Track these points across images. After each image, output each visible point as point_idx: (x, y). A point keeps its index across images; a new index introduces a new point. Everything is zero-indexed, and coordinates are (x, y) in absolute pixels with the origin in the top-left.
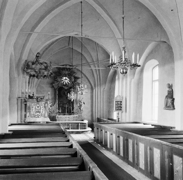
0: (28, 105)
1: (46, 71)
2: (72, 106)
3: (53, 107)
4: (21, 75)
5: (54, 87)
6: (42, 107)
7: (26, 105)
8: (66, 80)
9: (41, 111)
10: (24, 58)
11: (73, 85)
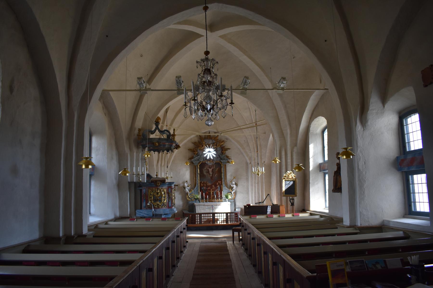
0: (144, 191)
1: (167, 142)
4: (135, 150)
5: (193, 163)
6: (163, 193)
7: (141, 190)
8: (210, 153)
9: (163, 199)
10: (139, 124)
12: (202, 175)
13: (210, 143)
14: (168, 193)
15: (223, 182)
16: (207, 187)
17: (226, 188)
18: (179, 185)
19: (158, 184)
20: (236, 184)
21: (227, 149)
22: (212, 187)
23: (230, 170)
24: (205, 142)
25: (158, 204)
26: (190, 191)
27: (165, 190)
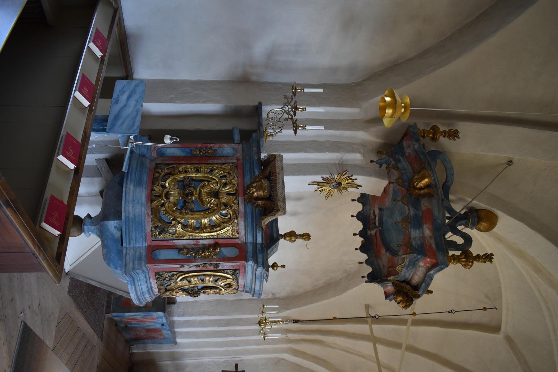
0: (227, 149)
14: (216, 245)
19: (260, 188)
25: (168, 195)
27: (227, 231)
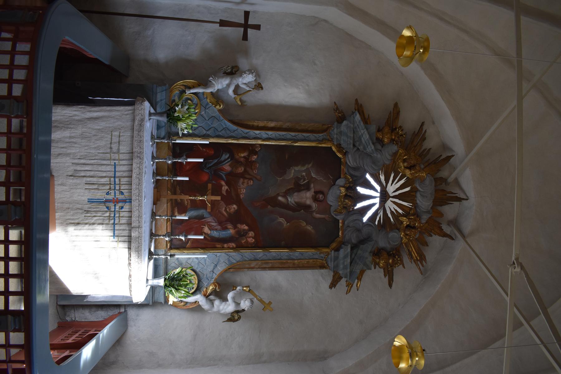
2: (215, 234)
3: (215, 110)
5: (341, 120)
11: (354, 241)
12: (284, 157)
13: (419, 199)
15: (247, 253)
16: (232, 179)
17: (220, 268)
18: (246, 53)
20: (234, 317)
21: (389, 274)
22: (228, 199)
23: (302, 286)
24: (422, 180)
26: (217, 97)
